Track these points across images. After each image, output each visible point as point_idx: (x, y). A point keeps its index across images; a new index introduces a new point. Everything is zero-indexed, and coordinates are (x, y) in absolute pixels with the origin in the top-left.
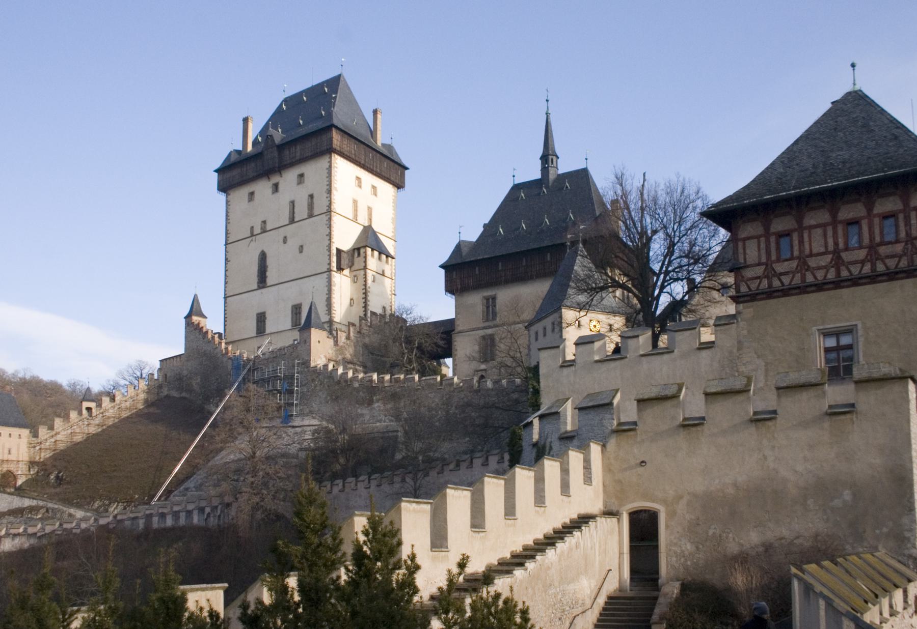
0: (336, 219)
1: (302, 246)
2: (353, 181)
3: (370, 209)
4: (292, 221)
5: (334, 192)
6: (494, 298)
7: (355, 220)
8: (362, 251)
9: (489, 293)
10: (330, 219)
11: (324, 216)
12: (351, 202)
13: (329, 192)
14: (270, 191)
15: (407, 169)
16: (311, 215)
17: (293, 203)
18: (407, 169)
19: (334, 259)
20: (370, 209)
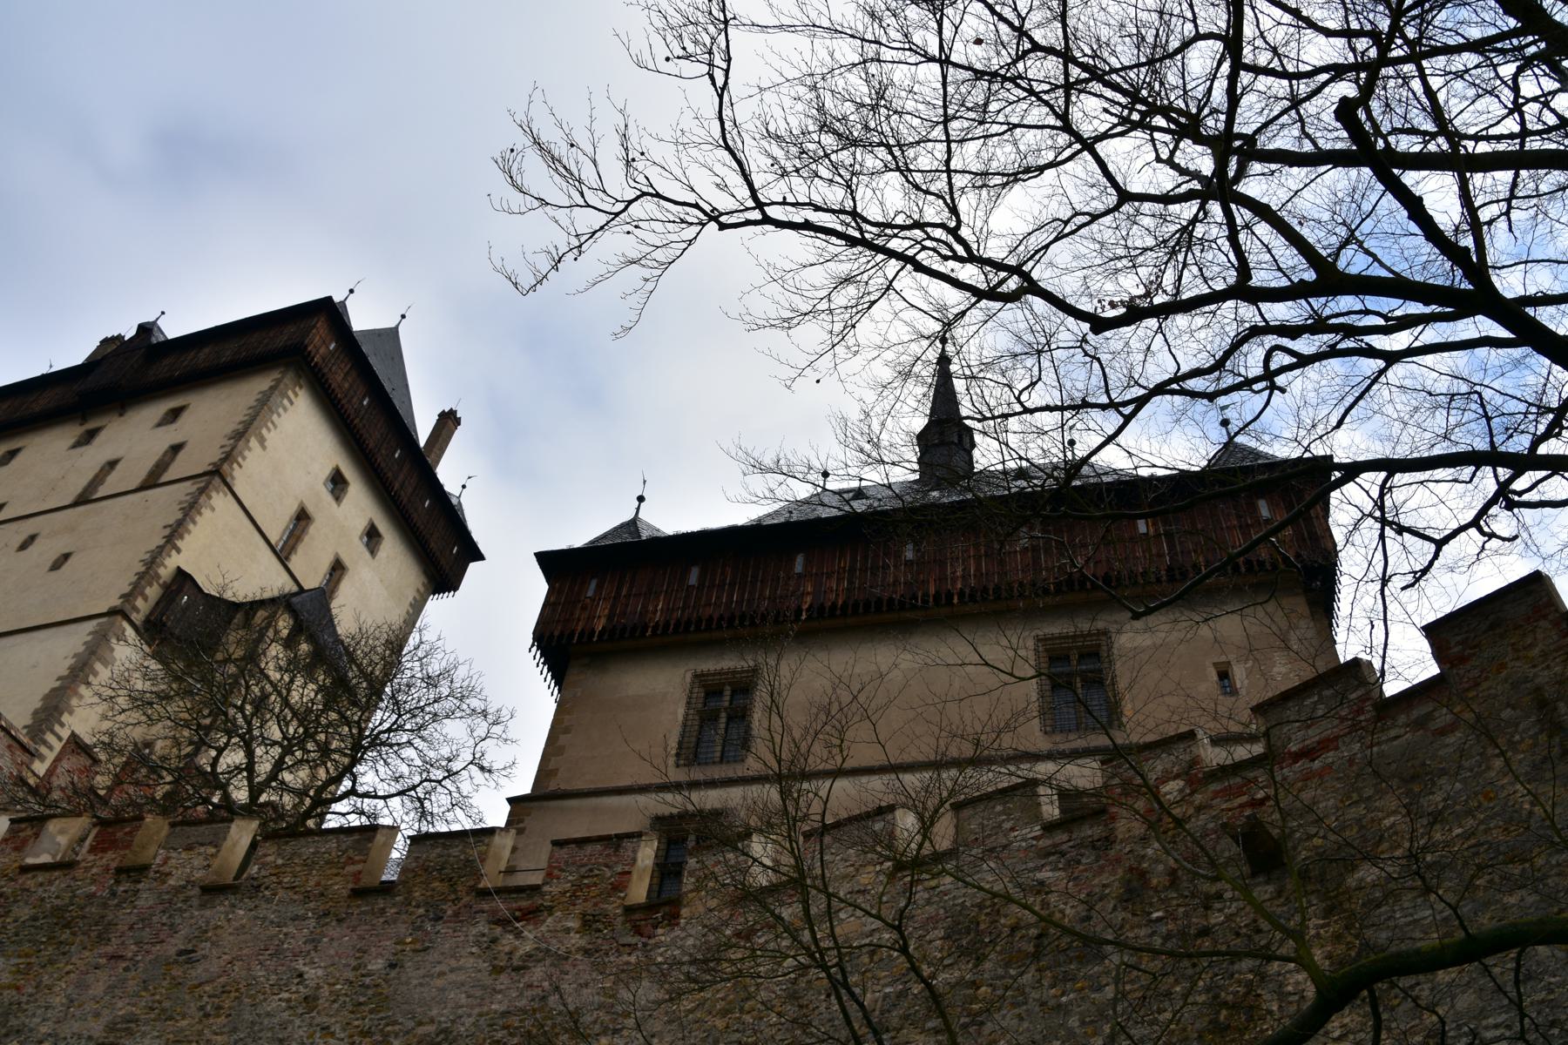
0: (220, 501)
1: (66, 556)
2: (327, 472)
3: (338, 569)
4: (83, 500)
5: (254, 443)
6: (743, 686)
7: (283, 555)
8: (261, 614)
9: (728, 662)
10: (202, 491)
11: (188, 484)
12: (291, 509)
13: (240, 435)
14: (72, 441)
15: (481, 557)
16: (152, 482)
17: (112, 464)
18: (481, 557)
19: (153, 592)
20: (338, 569)
